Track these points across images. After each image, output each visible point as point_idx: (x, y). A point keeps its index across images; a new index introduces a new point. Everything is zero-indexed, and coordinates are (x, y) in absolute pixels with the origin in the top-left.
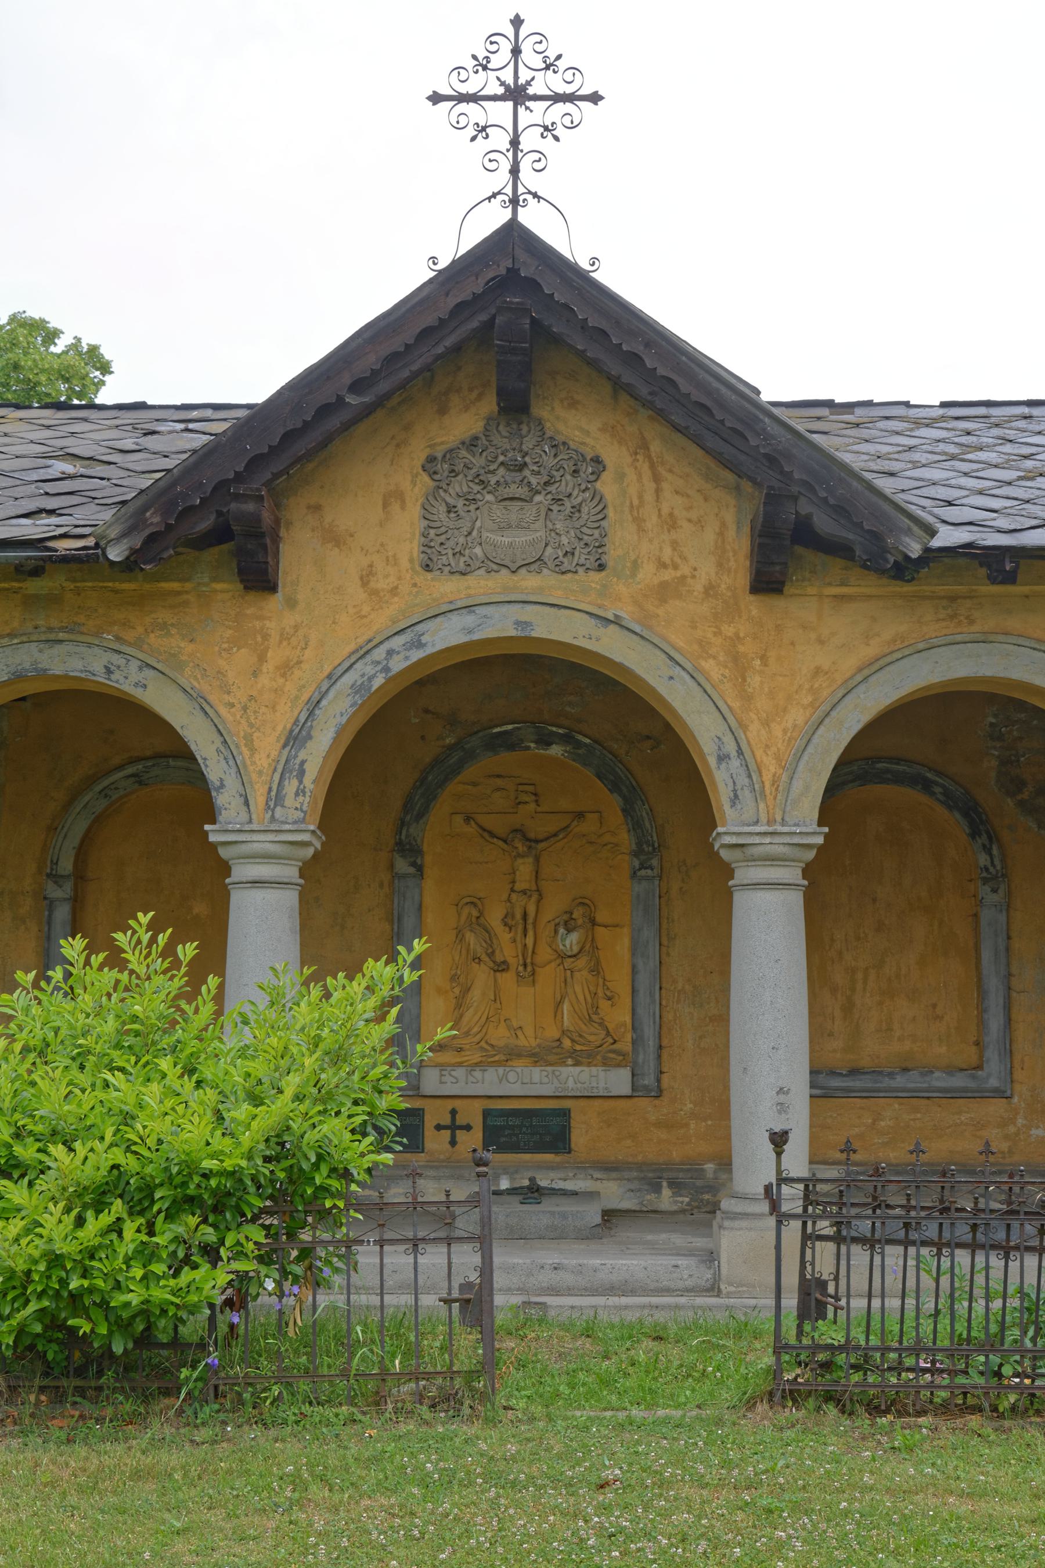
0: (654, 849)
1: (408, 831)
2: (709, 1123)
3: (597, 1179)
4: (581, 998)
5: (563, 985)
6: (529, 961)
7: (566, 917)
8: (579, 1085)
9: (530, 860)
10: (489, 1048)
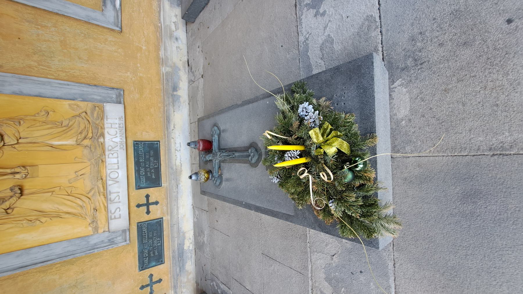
2: (139, 65)
6: (9, 171)
10: (93, 192)
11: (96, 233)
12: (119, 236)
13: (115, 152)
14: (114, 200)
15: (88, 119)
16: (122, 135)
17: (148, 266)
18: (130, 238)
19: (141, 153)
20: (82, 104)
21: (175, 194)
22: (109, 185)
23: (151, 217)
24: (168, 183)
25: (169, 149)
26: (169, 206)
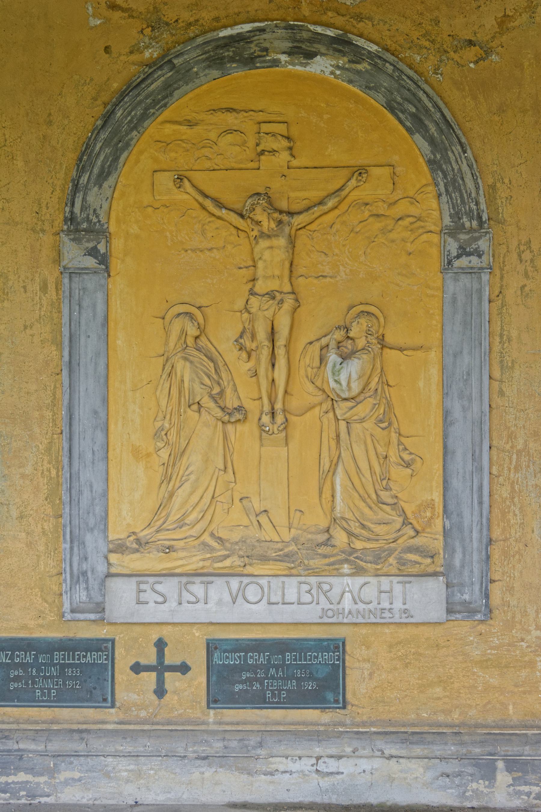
0: (481, 223)
1: (84, 200)
3: (392, 757)
4: (364, 465)
5: (333, 444)
6: (279, 406)
7: (339, 335)
8: (361, 606)
9: (282, 242)
11: (111, 546)
12: (89, 596)
13: (315, 596)
14: (188, 591)
15: (400, 541)
16: (360, 616)
18: (78, 620)
19: (310, 656)
21: (181, 751)
22: (228, 583)
24: (215, 727)
26: (146, 727)
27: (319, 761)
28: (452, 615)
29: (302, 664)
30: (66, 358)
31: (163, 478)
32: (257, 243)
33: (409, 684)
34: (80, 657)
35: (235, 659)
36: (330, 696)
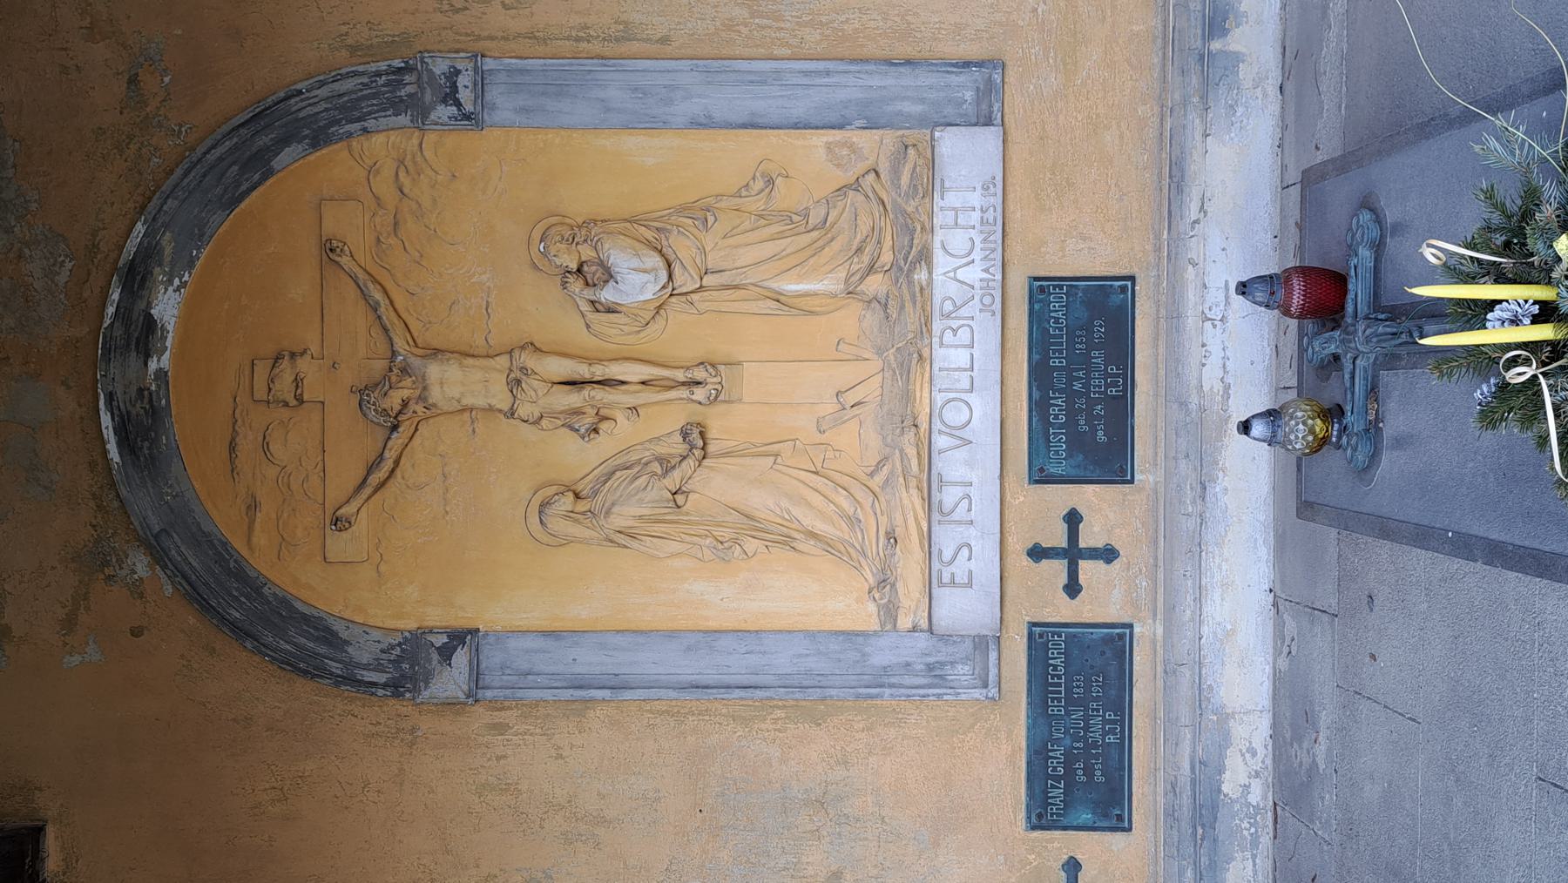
0: (408, 69)
1: (366, 667)
4: (770, 248)
6: (680, 376)
7: (576, 285)
9: (434, 371)
11: (888, 627)
13: (961, 322)
16: (992, 256)
17: (1065, 822)
20: (866, 140)
21: (1191, 524)
23: (1082, 610)
25: (1174, 317)
26: (1161, 576)
27: (1209, 316)
28: (994, 117)
29: (1066, 342)
30: (606, 693)
31: (788, 548)
32: (434, 405)
33: (1100, 180)
34: (1055, 675)
35: (1059, 441)
36: (1116, 299)
